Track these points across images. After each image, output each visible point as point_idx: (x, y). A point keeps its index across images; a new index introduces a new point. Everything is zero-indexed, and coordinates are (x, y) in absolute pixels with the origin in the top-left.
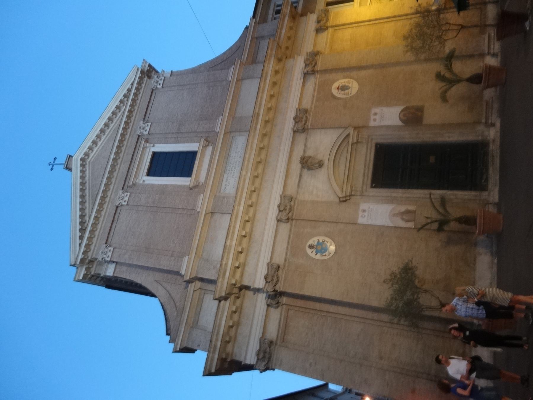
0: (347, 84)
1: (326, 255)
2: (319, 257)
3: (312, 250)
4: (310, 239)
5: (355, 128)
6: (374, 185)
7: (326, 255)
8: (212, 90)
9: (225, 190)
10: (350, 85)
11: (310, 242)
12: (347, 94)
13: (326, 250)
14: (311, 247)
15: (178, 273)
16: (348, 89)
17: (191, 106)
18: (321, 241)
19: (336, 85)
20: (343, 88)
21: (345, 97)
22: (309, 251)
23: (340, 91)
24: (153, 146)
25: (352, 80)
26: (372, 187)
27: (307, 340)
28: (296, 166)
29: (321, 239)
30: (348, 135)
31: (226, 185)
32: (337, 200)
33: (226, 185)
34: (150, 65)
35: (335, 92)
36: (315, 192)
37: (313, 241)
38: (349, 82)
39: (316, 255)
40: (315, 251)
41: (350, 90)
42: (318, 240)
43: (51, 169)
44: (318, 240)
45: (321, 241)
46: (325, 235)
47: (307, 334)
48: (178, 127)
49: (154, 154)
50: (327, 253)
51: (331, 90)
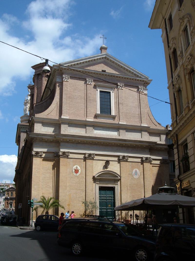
2: (74, 170)
4: (79, 166)
5: (120, 179)
8: (137, 116)
15: (61, 113)
17: (131, 107)
19: (137, 170)
21: (133, 174)
24: (113, 92)
26: (99, 187)
27: (44, 168)
30: (117, 177)
32: (94, 175)
34: (149, 84)
35: (134, 170)
36: (97, 166)
41: (135, 175)
43: (101, 37)
47: (46, 168)
48: (121, 103)
49: (110, 92)
51: (136, 168)
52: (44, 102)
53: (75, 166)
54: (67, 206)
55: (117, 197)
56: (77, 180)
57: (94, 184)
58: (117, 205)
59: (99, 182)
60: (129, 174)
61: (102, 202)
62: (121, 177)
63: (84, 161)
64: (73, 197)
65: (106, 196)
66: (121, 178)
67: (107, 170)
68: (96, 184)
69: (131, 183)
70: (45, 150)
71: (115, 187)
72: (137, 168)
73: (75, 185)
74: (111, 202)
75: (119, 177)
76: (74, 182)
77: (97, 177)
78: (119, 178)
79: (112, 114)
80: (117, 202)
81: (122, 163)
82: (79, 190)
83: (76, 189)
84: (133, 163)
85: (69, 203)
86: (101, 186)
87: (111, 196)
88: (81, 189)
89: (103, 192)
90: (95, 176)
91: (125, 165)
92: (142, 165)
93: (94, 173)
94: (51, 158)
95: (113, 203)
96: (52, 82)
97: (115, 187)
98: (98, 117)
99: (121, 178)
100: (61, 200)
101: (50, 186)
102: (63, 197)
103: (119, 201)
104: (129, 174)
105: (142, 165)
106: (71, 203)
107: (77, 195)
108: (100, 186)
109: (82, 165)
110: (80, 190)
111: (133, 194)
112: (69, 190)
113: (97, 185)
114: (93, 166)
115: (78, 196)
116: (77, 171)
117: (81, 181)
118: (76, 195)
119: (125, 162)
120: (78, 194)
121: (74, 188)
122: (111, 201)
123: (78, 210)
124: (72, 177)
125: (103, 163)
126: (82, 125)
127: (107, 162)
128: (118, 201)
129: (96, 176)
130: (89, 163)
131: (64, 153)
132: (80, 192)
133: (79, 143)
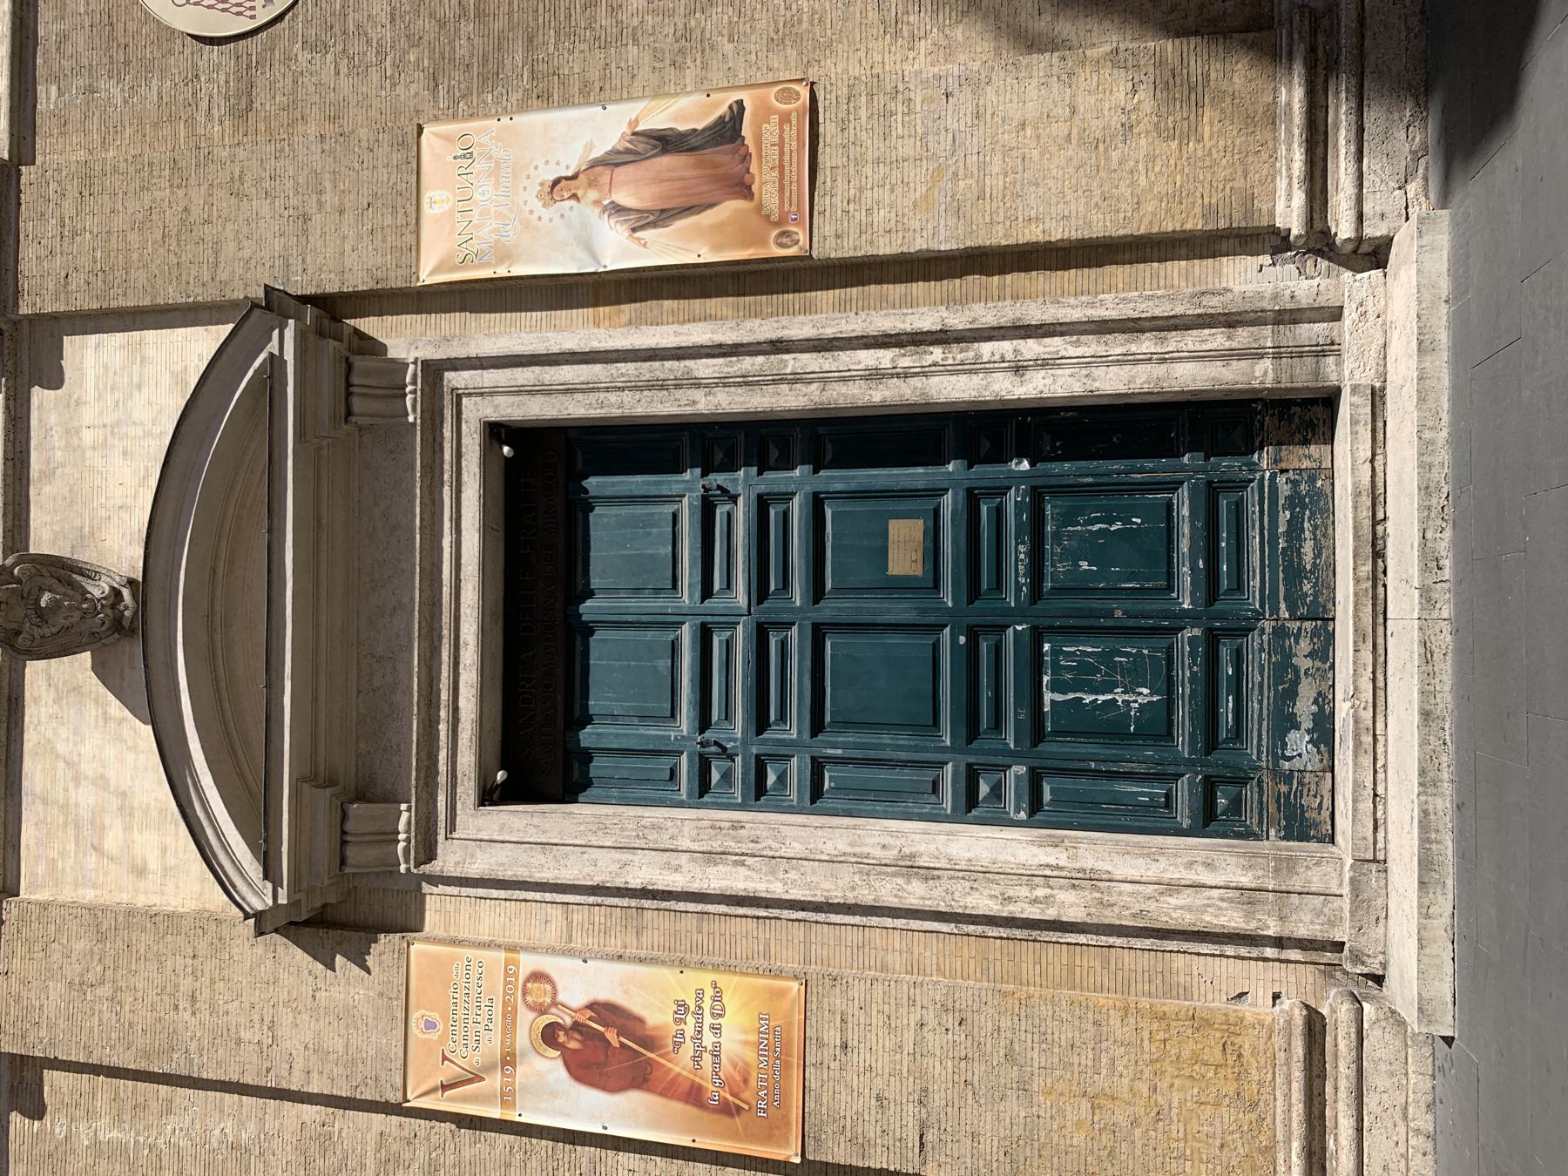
6: (501, 776)
26: (489, 796)
55: (704, 368)
57: (438, 907)
58: (875, 375)
59: (392, 798)
60: (242, 109)
61: (817, 727)
62: (275, 304)
63: (37, 1111)
65: (687, 634)
66: (300, 285)
69: (414, 41)
74: (817, 503)
78: (285, 342)
80: (824, 379)
86: (467, 759)
87: (688, 510)
91: (68, 207)
95: (836, 479)
97: (495, 432)
99: (305, 299)
103: (800, 328)
104: (242, 109)
108: (468, 790)
113: (449, 859)
128: (793, 362)
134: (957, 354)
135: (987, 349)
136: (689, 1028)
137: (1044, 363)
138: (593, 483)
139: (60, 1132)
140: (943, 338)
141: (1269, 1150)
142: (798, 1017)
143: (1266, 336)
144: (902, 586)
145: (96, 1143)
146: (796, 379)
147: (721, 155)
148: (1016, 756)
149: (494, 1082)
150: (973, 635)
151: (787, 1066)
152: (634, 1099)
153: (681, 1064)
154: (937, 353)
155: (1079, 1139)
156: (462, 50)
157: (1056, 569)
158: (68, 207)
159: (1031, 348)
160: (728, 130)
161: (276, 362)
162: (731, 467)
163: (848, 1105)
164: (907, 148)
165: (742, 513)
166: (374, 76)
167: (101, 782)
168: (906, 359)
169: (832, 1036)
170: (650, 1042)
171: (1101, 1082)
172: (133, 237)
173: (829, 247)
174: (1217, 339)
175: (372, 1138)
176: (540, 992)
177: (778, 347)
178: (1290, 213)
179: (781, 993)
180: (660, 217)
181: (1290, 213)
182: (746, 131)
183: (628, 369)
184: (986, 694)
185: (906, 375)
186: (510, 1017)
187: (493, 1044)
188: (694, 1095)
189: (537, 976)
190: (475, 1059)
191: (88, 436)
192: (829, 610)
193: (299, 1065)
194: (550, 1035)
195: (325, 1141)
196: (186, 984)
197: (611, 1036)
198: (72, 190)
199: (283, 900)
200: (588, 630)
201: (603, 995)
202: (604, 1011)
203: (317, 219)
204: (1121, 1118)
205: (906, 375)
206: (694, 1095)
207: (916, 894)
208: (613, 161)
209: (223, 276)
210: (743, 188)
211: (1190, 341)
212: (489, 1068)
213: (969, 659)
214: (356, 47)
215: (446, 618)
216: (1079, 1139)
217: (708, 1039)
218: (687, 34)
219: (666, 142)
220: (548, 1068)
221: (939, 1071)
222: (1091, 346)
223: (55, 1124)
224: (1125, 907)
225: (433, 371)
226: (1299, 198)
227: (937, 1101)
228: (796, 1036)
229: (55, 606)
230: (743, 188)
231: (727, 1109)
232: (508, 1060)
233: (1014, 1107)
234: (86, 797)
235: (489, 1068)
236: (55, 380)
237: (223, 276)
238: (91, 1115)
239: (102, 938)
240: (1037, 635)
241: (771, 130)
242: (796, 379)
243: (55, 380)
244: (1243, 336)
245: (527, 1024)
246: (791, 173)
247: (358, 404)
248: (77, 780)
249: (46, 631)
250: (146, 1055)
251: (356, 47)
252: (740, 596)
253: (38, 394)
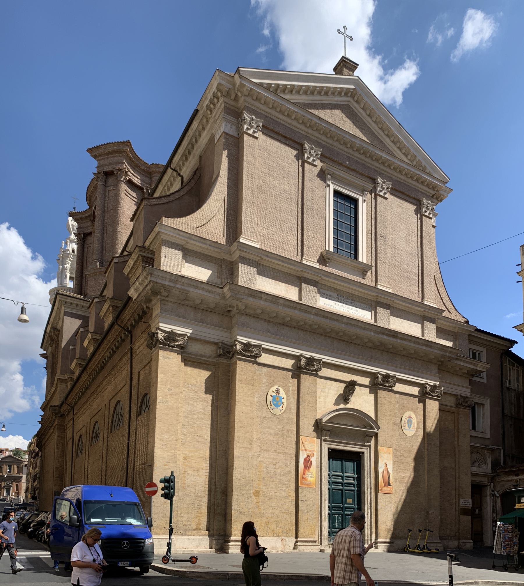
0: (412, 425)
1: (271, 405)
3: (275, 392)
4: (284, 390)
7: (271, 405)
9: (323, 293)
10: (411, 429)
11: (282, 391)
12: (405, 425)
13: (277, 406)
14: (278, 392)
16: (408, 426)
18: (283, 400)
19: (413, 415)
20: (410, 422)
22: (274, 388)
23: (408, 419)
25: (415, 430)
26: (329, 449)
28: (348, 377)
29: (285, 401)
31: (327, 295)
32: (318, 417)
33: (327, 295)
37: (282, 394)
38: (414, 427)
39: (271, 395)
40: (274, 394)
41: (407, 428)
42: (284, 398)
44: (284, 398)
45: (283, 400)
46: (287, 404)
50: (273, 406)
51: (408, 410)
52: (171, 201)
53: (272, 386)
54: (253, 496)
55: (369, 479)
56: (279, 427)
58: (368, 499)
59: (329, 437)
61: (333, 489)
63: (292, 377)
64: (267, 473)
65: (341, 474)
67: (348, 406)
68: (323, 443)
69: (399, 447)
70: (188, 331)
71: (363, 453)
72: (412, 410)
73: (271, 438)
74: (353, 491)
75: (376, 429)
76: (271, 431)
77: (326, 422)
79: (360, 260)
80: (367, 493)
81: (382, 394)
82: (283, 453)
83: (275, 450)
84: (404, 397)
85: (257, 490)
87: (352, 475)
88: (287, 451)
89: (337, 464)
90: (321, 419)
91: (388, 399)
92: (422, 404)
93: (318, 411)
94: (208, 357)
96: (193, 147)
97: (363, 453)
98: (328, 263)
100: (239, 477)
101: (206, 437)
102: (242, 471)
104: (395, 424)
105: (422, 404)
106: (264, 488)
107: (277, 467)
109: (291, 388)
110: (285, 453)
111: (403, 475)
112: (258, 453)
113: (323, 443)
114: (315, 392)
115: (279, 470)
116: (277, 401)
117: (288, 431)
118: (275, 468)
119: (387, 393)
120: (280, 464)
121: (270, 449)
122: (353, 488)
123: (280, 508)
124: (265, 418)
125: (340, 388)
126: (290, 275)
127: (350, 387)
128: (369, 490)
129: (324, 420)
130: (308, 384)
131: (247, 346)
132: (285, 459)
133: (284, 324)
134: (369, 508)
135: (369, 511)
136: (310, 474)
137: (368, 517)
138: (355, 463)
139: (290, 381)
140: (371, 506)
141: (305, 537)
142: (312, 487)
143: (369, 538)
144: (346, 500)
145: (289, 387)
146: (367, 490)
147: (387, 484)
148: (331, 512)
149: (303, 448)
150: (342, 508)
151: (307, 485)
152: (303, 466)
153: (307, 473)
154: (369, 506)
155: (304, 518)
156: (398, 453)
157: (348, 517)
158: (388, 399)
159: (369, 515)
160: (389, 485)
161: (374, 429)
162: (357, 481)
163: (304, 492)
164: (387, 504)
165: (352, 482)
166: (396, 442)
167: (328, 393)
168: (369, 502)
169: (311, 491)
170: (309, 468)
171: (309, 520)
172: (384, 408)
173: (380, 495)
174: (369, 534)
175: (293, 429)
176: (312, 455)
177: (371, 488)
178: (379, 540)
179: (314, 484)
180: (383, 476)
181: (379, 540)
182: (389, 486)
183: (369, 471)
184: (336, 509)
185: (367, 502)
186: (310, 451)
187: (307, 449)
188: (304, 474)
189: (314, 455)
190: (306, 446)
191: (364, 396)
192: (344, 491)
193: (303, 421)
194: (308, 456)
195: (293, 422)
196: (310, 405)
197: (309, 464)
198: (389, 400)
199: (323, 423)
200: (341, 461)
201: (313, 463)
202: (311, 463)
203: (385, 433)
204: (306, 522)
205: (367, 502)
206: (304, 474)
207: (323, 501)
208: (388, 471)
209: (380, 420)
210: (384, 486)
211: (369, 531)
212: (305, 447)
213: (339, 507)
214: (399, 439)
215: (346, 445)
216: (304, 518)
217: (309, 476)
218: (397, 480)
219: (389, 477)
220: (305, 456)
221: (308, 503)
222: (369, 521)
223: (291, 380)
224: (323, 523)
225: (370, 446)
226: (381, 541)
227: (306, 502)
228: (310, 486)
229: (350, 393)
230: (384, 486)
231: (303, 477)
232: (306, 450)
233: (306, 511)
234: (327, 390)
235: (305, 447)
236: (370, 393)
237: (380, 420)
238: (293, 386)
239: (314, 393)
240: (342, 515)
241: (389, 489)
242: (367, 490)
243: (370, 393)
244: (369, 536)
245: (309, 453)
246: (386, 491)
247: (368, 437)
248: (329, 389)
249: (347, 391)
250: (302, 398)
251: (399, 439)
252: (345, 481)
253: (368, 389)
